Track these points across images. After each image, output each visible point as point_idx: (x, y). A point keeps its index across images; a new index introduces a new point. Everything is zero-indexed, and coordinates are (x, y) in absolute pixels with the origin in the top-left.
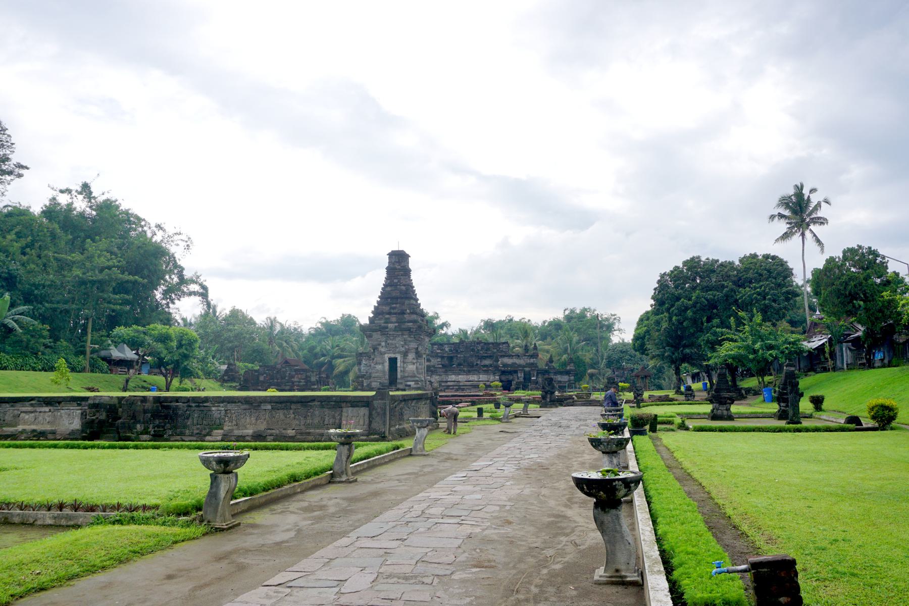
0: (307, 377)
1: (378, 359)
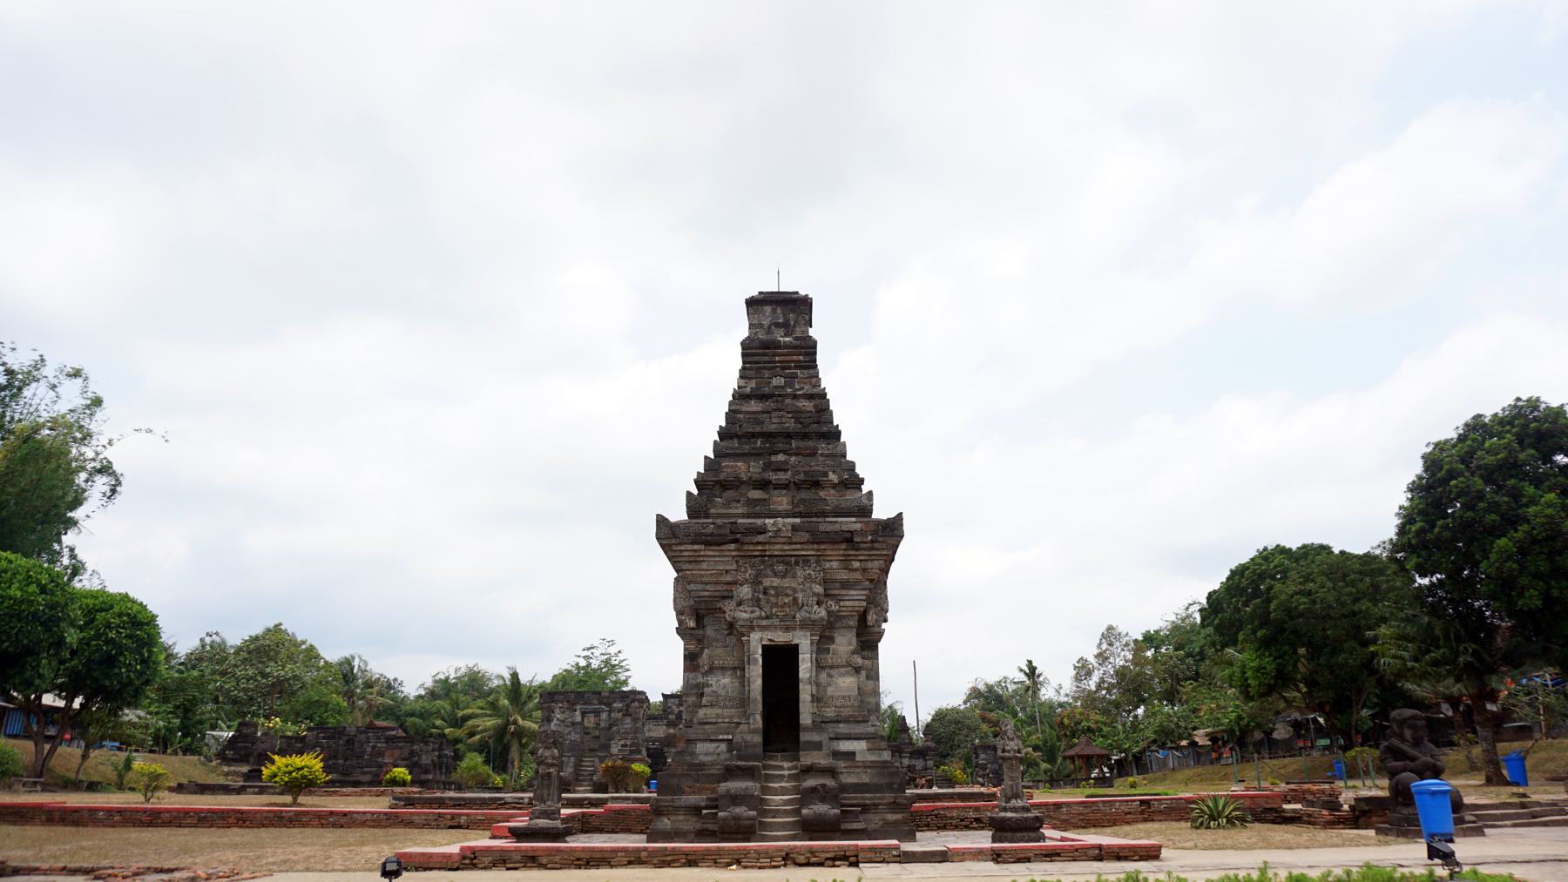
0: (412, 753)
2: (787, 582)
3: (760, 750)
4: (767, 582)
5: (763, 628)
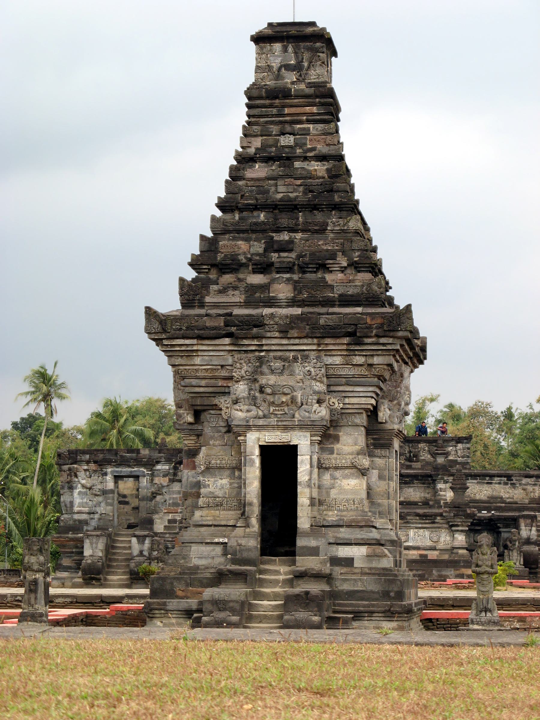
1: (213, 451)
2: (283, 380)
3: (255, 554)
4: (263, 380)
5: (260, 428)
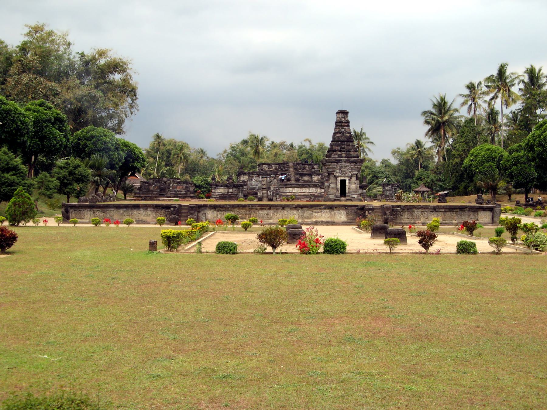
1: (332, 180)
2: (345, 170)
